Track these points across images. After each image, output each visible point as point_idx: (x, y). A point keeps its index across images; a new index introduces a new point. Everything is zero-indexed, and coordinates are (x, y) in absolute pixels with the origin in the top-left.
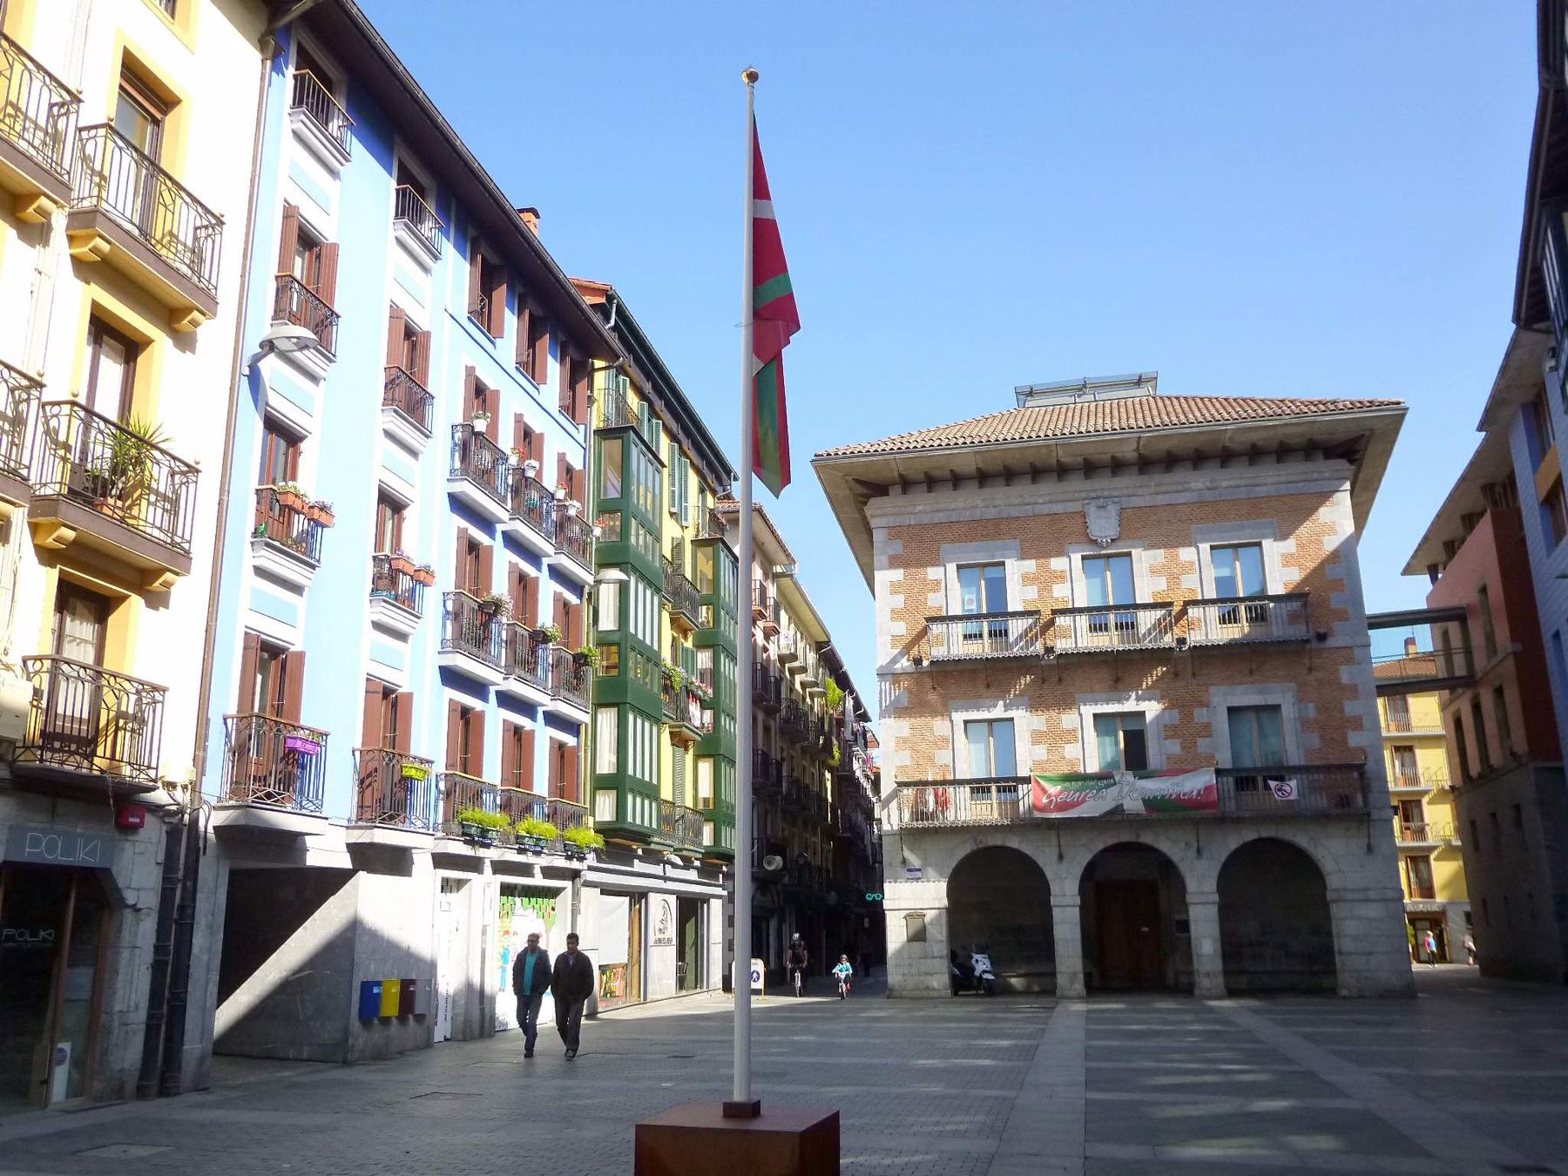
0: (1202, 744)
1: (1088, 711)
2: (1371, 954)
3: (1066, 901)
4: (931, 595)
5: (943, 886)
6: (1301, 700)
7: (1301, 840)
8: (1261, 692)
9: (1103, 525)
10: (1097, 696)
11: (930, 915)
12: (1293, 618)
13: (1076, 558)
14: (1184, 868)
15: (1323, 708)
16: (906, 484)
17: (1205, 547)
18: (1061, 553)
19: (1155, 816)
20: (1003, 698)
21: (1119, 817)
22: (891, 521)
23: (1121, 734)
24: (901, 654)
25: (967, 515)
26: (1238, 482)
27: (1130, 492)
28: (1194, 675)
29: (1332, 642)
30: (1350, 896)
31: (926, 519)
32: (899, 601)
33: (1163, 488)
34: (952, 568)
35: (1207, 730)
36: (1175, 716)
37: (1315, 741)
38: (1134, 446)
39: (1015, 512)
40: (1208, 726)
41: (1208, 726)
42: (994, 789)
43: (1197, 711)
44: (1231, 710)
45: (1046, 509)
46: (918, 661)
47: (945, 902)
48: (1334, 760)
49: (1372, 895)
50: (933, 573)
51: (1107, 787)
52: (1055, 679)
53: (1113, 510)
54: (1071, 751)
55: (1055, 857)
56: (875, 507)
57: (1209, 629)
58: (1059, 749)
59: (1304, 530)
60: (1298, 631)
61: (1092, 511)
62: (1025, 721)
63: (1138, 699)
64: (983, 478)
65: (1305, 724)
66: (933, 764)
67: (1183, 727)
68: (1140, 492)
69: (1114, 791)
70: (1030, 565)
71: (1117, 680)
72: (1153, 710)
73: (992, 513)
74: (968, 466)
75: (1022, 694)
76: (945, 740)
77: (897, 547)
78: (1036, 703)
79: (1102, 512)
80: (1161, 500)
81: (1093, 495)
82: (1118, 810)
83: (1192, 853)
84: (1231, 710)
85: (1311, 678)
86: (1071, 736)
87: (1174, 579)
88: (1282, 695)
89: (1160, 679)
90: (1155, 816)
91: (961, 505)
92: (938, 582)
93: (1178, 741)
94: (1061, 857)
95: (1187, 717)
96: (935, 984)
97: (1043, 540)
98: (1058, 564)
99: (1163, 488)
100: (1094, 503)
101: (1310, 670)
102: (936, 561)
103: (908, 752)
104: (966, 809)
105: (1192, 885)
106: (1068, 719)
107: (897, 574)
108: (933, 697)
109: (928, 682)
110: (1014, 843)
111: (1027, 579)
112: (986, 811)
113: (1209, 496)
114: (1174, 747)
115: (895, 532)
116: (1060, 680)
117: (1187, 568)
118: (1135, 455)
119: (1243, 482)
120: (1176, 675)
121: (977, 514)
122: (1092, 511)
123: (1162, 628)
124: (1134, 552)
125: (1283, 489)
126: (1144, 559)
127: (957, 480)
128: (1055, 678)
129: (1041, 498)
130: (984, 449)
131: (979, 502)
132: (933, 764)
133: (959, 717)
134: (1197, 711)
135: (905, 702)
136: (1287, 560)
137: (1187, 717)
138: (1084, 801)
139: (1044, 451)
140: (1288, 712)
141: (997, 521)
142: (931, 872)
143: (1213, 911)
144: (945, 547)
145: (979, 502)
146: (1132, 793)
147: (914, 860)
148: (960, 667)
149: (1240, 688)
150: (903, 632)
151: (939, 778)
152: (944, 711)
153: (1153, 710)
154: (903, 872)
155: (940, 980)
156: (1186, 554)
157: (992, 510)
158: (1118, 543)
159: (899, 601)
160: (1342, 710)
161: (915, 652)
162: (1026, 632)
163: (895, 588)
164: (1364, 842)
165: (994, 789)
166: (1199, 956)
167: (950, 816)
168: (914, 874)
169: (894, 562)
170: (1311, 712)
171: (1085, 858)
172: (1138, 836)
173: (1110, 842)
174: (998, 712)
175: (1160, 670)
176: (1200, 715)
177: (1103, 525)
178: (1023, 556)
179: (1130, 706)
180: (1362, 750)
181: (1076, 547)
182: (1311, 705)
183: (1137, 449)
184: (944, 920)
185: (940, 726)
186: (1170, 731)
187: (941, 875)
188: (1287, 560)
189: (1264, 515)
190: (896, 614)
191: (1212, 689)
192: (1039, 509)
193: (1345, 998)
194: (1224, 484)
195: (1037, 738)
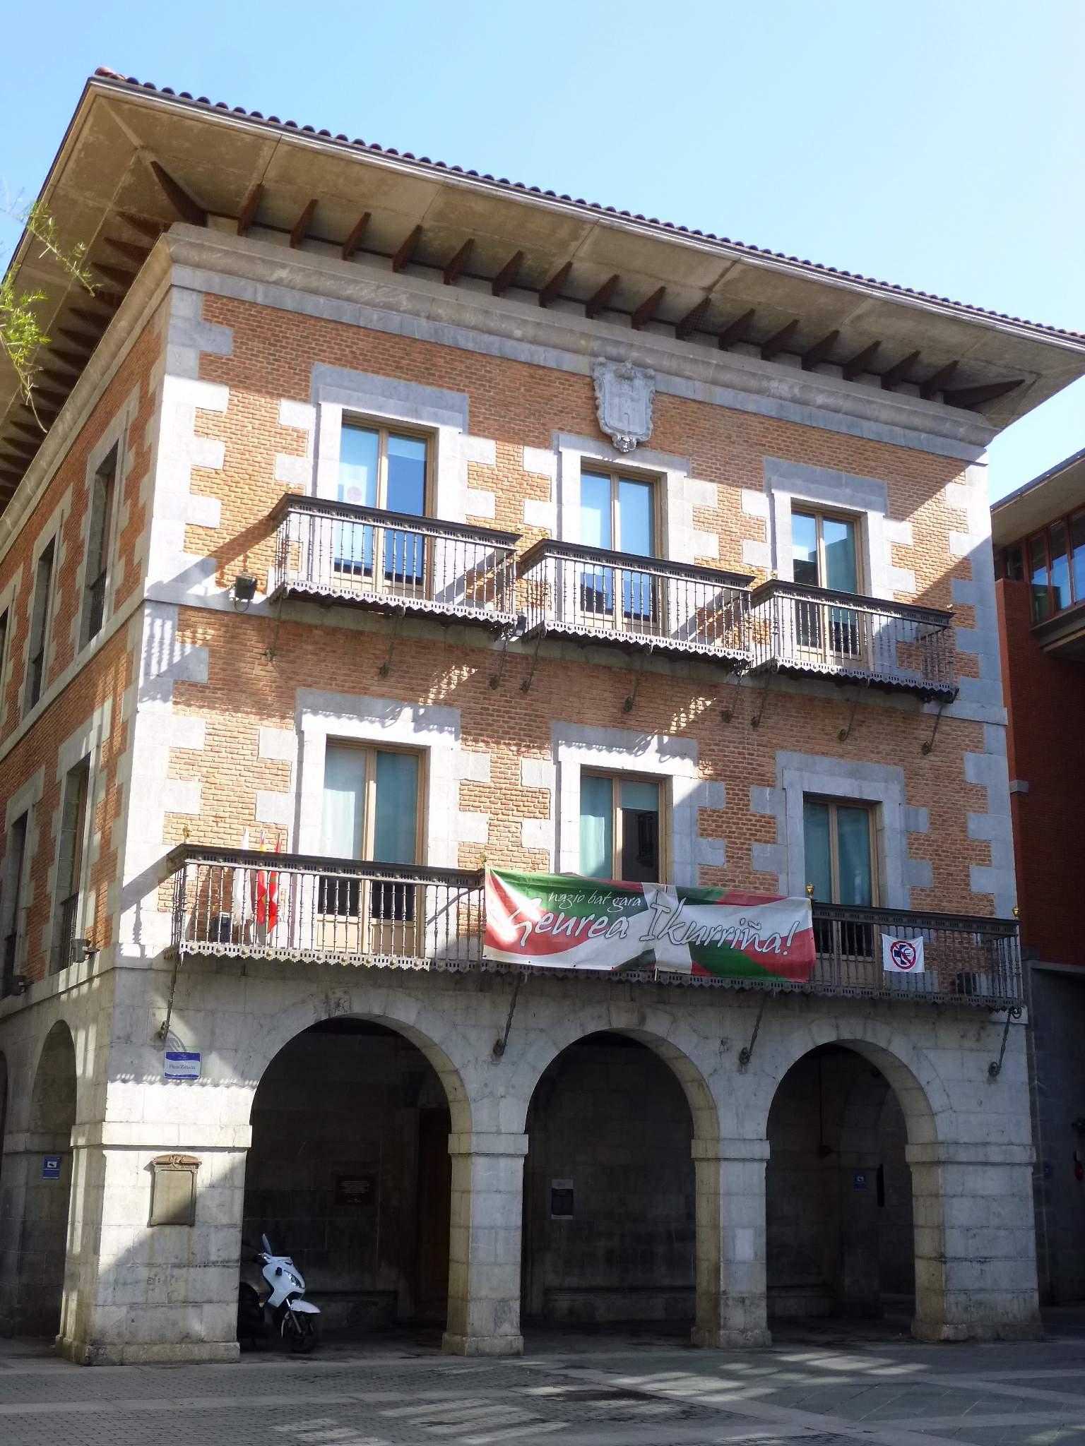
0: (761, 854)
1: (575, 757)
2: (984, 1260)
3: (502, 1145)
4: (281, 459)
5: (245, 1097)
6: (909, 800)
7: (899, 1047)
8: (853, 774)
9: (626, 410)
10: (590, 731)
11: (212, 1168)
12: (906, 652)
13: (573, 458)
14: (717, 1087)
15: (939, 820)
16: (253, 219)
17: (784, 499)
18: (543, 441)
19: (706, 980)
20: (413, 702)
21: (643, 977)
22: (217, 283)
23: (619, 814)
24: (204, 568)
25: (373, 319)
26: (841, 403)
27: (672, 364)
28: (755, 724)
29: (958, 709)
30: (963, 1156)
31: (290, 301)
32: (213, 453)
33: (726, 377)
34: (332, 413)
35: (767, 828)
36: (719, 797)
37: (926, 876)
38: (707, 282)
39: (467, 341)
40: (770, 821)
41: (769, 822)
42: (366, 889)
43: (754, 791)
44: (809, 798)
45: (524, 352)
46: (246, 587)
47: (245, 1138)
48: (950, 907)
49: (995, 1155)
50: (293, 413)
51: (629, 912)
52: (517, 683)
54: (536, 833)
55: (486, 1051)
56: (179, 240)
57: (783, 640)
58: (514, 824)
59: (925, 511)
60: (913, 675)
61: (607, 378)
62: (453, 761)
63: (662, 750)
64: (412, 256)
65: (914, 841)
66: (250, 822)
67: (726, 817)
68: (689, 369)
69: (640, 922)
70: (485, 450)
71: (628, 707)
72: (685, 777)
73: (421, 328)
74: (397, 218)
75: (447, 703)
76: (279, 770)
77: (221, 341)
78: (475, 728)
79: (626, 386)
80: (722, 396)
81: (613, 351)
82: (644, 962)
83: (732, 1059)
84: (809, 798)
85: (925, 763)
86: (539, 803)
87: (730, 542)
88: (879, 783)
89: (701, 718)
90: (706, 980)
91: (366, 293)
92: (301, 436)
93: (722, 842)
94: (499, 1049)
95: (738, 800)
96: (198, 1327)
97: (521, 409)
98: (536, 460)
99: (726, 377)
100: (613, 366)
101: (926, 749)
102: (301, 391)
103: (196, 786)
104: (310, 932)
105: (728, 1124)
106: (534, 769)
107: (217, 396)
108: (261, 672)
109: (254, 643)
110: (404, 1013)
111: (476, 476)
112: (349, 939)
113: (795, 413)
114: (715, 853)
115: (218, 308)
116: (525, 688)
117: (752, 528)
118: (696, 297)
119: (847, 405)
120: (727, 717)
121: (394, 323)
123: (710, 621)
124: (677, 480)
125: (900, 436)
126: (687, 493)
127: (358, 245)
128: (526, 678)
129: (519, 327)
130: (463, 192)
131: (405, 304)
132: (250, 822)
133: (320, 726)
134: (754, 791)
135: (201, 674)
136: (901, 556)
137: (738, 800)
138: (583, 937)
139: (563, 232)
140: (891, 817)
141: (431, 348)
142: (214, 1062)
143: (757, 1174)
144: (322, 371)
145: (405, 304)
146: (663, 931)
147: (183, 1035)
148: (332, 619)
149: (823, 763)
150: (215, 521)
151: (268, 848)
152: (284, 705)
153: (685, 777)
154: (154, 1059)
155: (216, 1319)
156: (753, 502)
157: (424, 322)
158: (649, 453)
159: (213, 453)
160: (964, 828)
161: (234, 568)
162: (470, 577)
163: (206, 424)
164: (985, 1060)
165: (366, 889)
166: (729, 1262)
167: (278, 942)
168: (182, 1065)
169: (211, 369)
170: (923, 825)
171: (541, 1056)
172: (643, 1020)
173: (591, 1028)
174: (400, 729)
175: (700, 704)
176: (761, 800)
177: (626, 410)
178: (475, 428)
179: (647, 761)
180: (986, 898)
181: (574, 438)
182: (924, 811)
183: (709, 289)
184: (240, 1180)
185: (274, 739)
186: (709, 820)
187: (244, 1076)
188: (901, 556)
189: (871, 472)
190: (203, 479)
191: (781, 756)
192: (511, 348)
193: (947, 1341)
194: (820, 399)
195: (471, 795)
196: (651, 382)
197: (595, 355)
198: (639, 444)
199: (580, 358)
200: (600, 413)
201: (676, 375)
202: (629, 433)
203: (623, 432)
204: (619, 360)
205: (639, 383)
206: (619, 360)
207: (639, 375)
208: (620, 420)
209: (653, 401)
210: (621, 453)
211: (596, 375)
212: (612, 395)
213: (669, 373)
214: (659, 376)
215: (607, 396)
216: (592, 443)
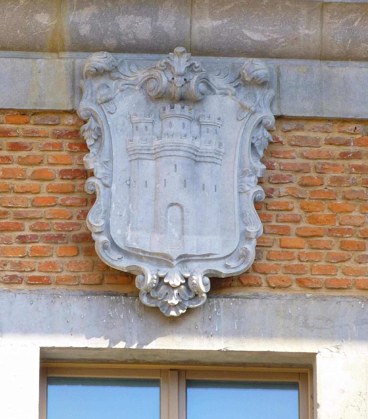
53: (230, 123)
61: (120, 111)
79: (176, 127)
100: (136, 71)
122: (120, 111)
158: (254, 306)
196: (265, 96)
197: (85, 47)
198: (219, 284)
199: (42, 62)
200: (95, 220)
201: (347, 57)
202: (185, 259)
203: (163, 260)
204: (157, 48)
205: (222, 105)
206: (157, 48)
207: (218, 82)
208: (157, 227)
209: (270, 152)
210: (162, 318)
211: (85, 106)
212: (135, 156)
213: (325, 57)
214: (291, 70)
215: (120, 163)
216: (77, 307)
